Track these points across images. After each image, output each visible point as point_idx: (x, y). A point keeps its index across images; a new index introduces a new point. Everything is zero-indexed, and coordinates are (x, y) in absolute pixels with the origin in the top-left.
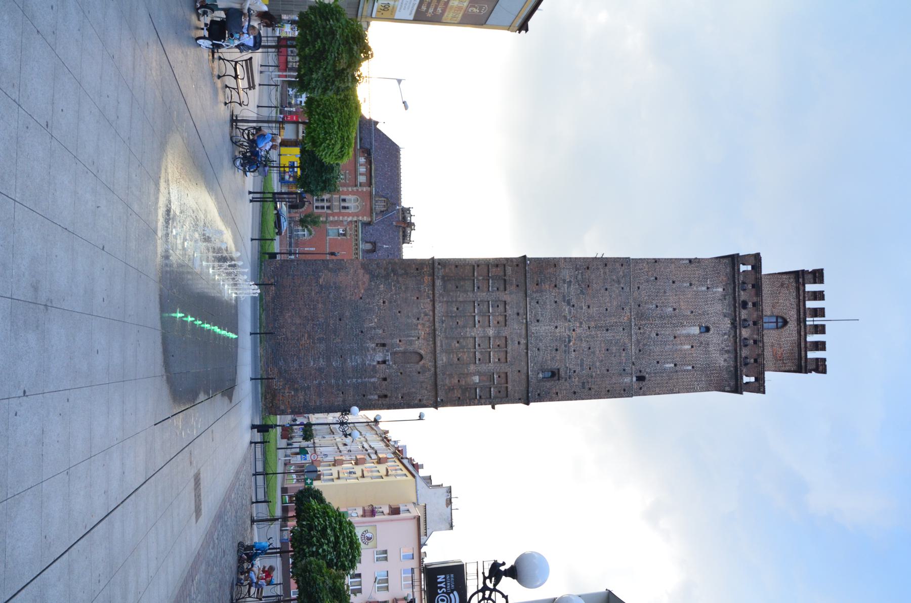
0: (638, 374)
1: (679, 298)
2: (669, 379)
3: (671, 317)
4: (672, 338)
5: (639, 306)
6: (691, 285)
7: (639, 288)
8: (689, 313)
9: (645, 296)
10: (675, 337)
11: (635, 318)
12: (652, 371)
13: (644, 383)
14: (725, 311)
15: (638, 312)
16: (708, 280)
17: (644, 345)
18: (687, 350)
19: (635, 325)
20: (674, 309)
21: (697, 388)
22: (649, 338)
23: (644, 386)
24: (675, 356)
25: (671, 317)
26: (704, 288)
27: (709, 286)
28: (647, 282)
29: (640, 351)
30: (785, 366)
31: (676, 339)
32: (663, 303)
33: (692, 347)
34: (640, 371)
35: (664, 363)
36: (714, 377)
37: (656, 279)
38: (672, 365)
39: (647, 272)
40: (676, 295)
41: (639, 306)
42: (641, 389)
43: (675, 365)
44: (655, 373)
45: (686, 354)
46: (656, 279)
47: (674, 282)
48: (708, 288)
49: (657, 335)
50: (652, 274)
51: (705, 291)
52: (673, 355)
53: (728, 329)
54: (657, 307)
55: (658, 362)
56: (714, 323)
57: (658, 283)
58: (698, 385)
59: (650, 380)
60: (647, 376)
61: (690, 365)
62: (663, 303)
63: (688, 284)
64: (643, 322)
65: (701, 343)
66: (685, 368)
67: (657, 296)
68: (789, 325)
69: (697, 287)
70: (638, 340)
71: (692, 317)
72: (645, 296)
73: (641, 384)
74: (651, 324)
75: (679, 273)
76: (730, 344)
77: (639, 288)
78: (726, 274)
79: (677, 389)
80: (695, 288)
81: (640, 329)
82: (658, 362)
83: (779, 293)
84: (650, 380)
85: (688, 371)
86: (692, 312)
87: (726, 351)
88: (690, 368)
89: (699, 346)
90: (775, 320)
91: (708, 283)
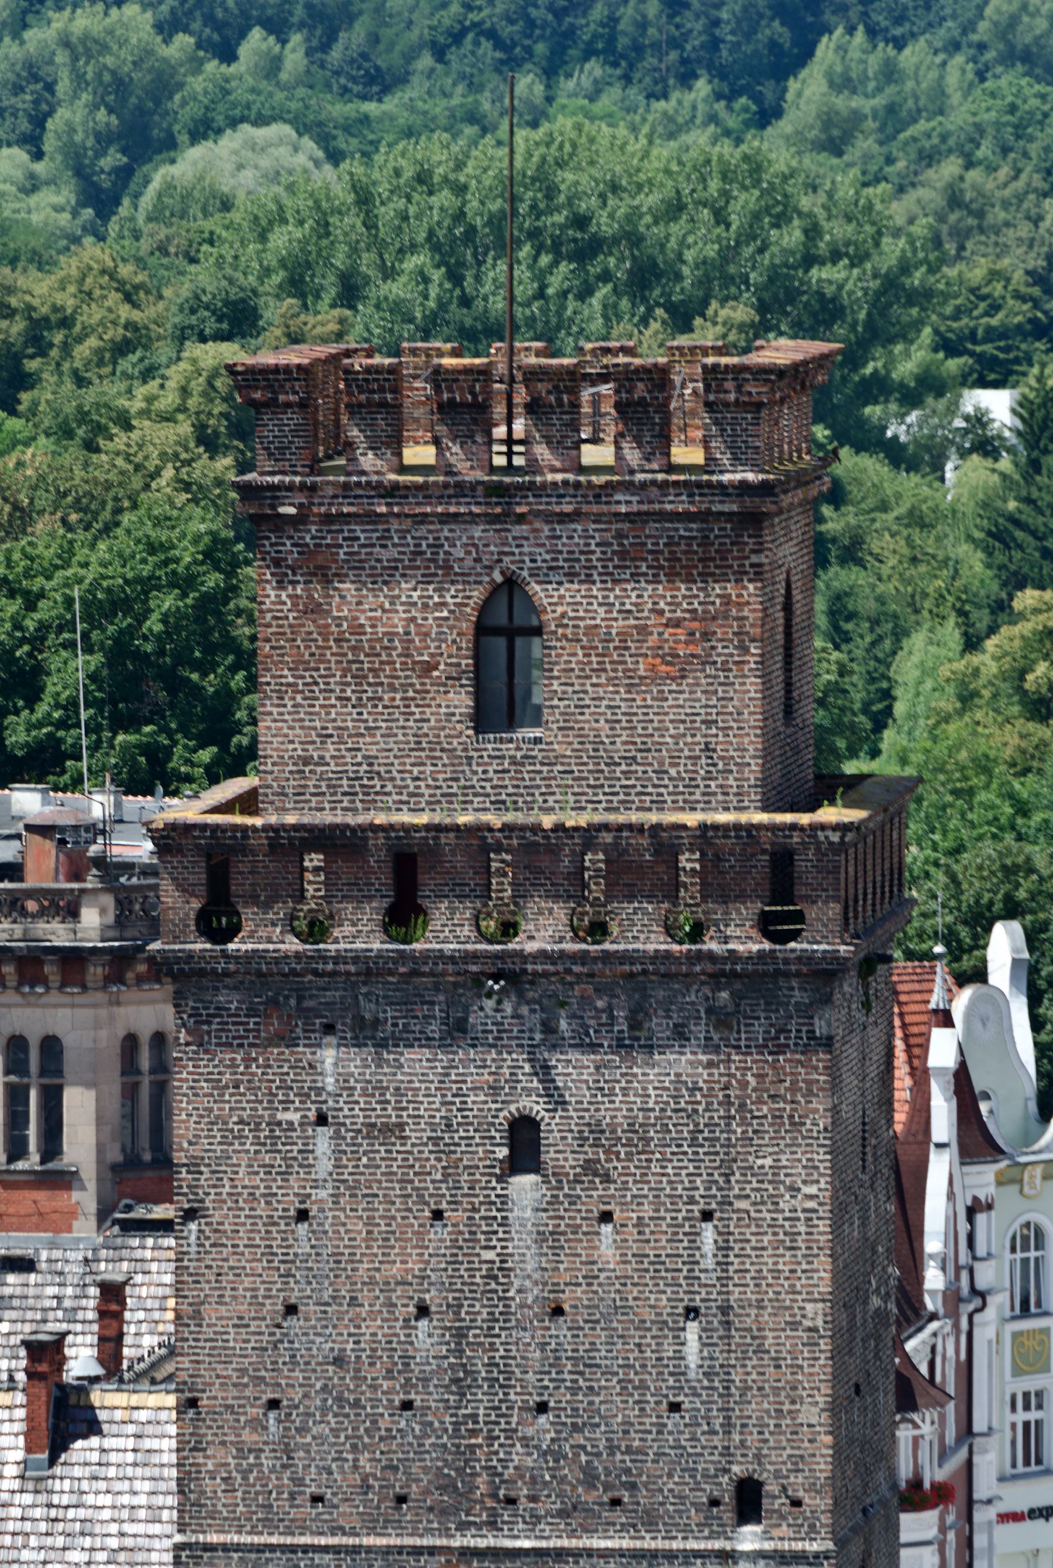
0: (728, 1516)
1: (372, 1282)
2: (760, 1350)
3: (460, 1334)
4: (561, 1330)
5: (401, 1499)
6: (303, 1215)
7: (317, 1499)
8: (440, 1233)
9: (356, 1467)
10: (558, 1311)
11: (463, 1526)
12: (716, 1441)
13: (772, 1487)
14: (434, 1029)
15: (431, 1509)
16: (280, 1116)
17: (590, 1478)
18: (621, 1245)
19: (493, 1525)
20: (423, 1311)
21: (811, 1197)
22: (559, 1455)
23: (784, 1489)
24: (649, 1316)
25: (460, 1334)
26: (323, 1141)
27: (312, 1115)
28: (288, 1452)
29: (616, 1502)
30: (740, 605)
31: (566, 1307)
32: (389, 1374)
33: (606, 1217)
34: (714, 1503)
35: (679, 1374)
36: (760, 1101)
37: (274, 1404)
38: (692, 1331)
39: (241, 1454)
40: (353, 1302)
41: (401, 1499)
42: (797, 1503)
43: (692, 1312)
44: (728, 1427)
45: (640, 1256)
46: (274, 1404)
47: (291, 1310)
48: (322, 1120)
49: (542, 1408)
50: (258, 1425)
51: (337, 1136)
52: (641, 1326)
53: (524, 1010)
54: (407, 1405)
55: (675, 1407)
56: (494, 1089)
57: (297, 1395)
58: (794, 1189)
59: (758, 1457)
60: (735, 1469)
61: (694, 1235)
62: (389, 1374)
63: (302, 1229)
64: (482, 1482)
65: (590, 1167)
66: (709, 1263)
67: (357, 1404)
68: (525, 573)
69: (316, 1184)
70: (563, 1514)
71: (461, 1215)
72: (356, 1467)
73: (773, 1502)
74: (491, 1438)
75: (247, 1282)
76: (600, 1004)
77: (317, 1499)
78: (252, 1012)
79: (809, 1307)
80: (323, 1194)
81: (511, 1501)
82: (675, 1407)
83: (358, 630)
84: (758, 1457)
85: (723, 1248)
86: (438, 1215)
87: (631, 1027)
88: (708, 1234)
89: (607, 1179)
90: (501, 642)
91: (295, 1117)
